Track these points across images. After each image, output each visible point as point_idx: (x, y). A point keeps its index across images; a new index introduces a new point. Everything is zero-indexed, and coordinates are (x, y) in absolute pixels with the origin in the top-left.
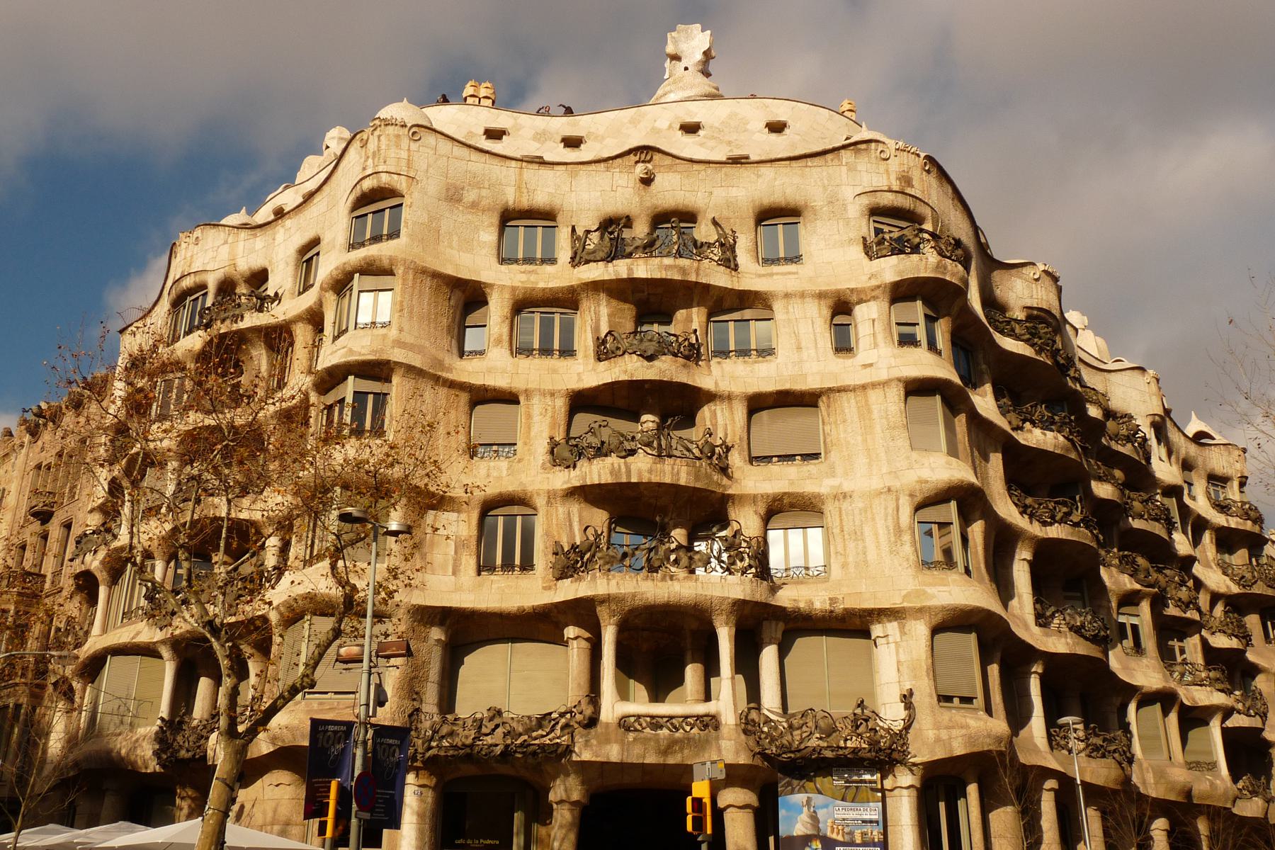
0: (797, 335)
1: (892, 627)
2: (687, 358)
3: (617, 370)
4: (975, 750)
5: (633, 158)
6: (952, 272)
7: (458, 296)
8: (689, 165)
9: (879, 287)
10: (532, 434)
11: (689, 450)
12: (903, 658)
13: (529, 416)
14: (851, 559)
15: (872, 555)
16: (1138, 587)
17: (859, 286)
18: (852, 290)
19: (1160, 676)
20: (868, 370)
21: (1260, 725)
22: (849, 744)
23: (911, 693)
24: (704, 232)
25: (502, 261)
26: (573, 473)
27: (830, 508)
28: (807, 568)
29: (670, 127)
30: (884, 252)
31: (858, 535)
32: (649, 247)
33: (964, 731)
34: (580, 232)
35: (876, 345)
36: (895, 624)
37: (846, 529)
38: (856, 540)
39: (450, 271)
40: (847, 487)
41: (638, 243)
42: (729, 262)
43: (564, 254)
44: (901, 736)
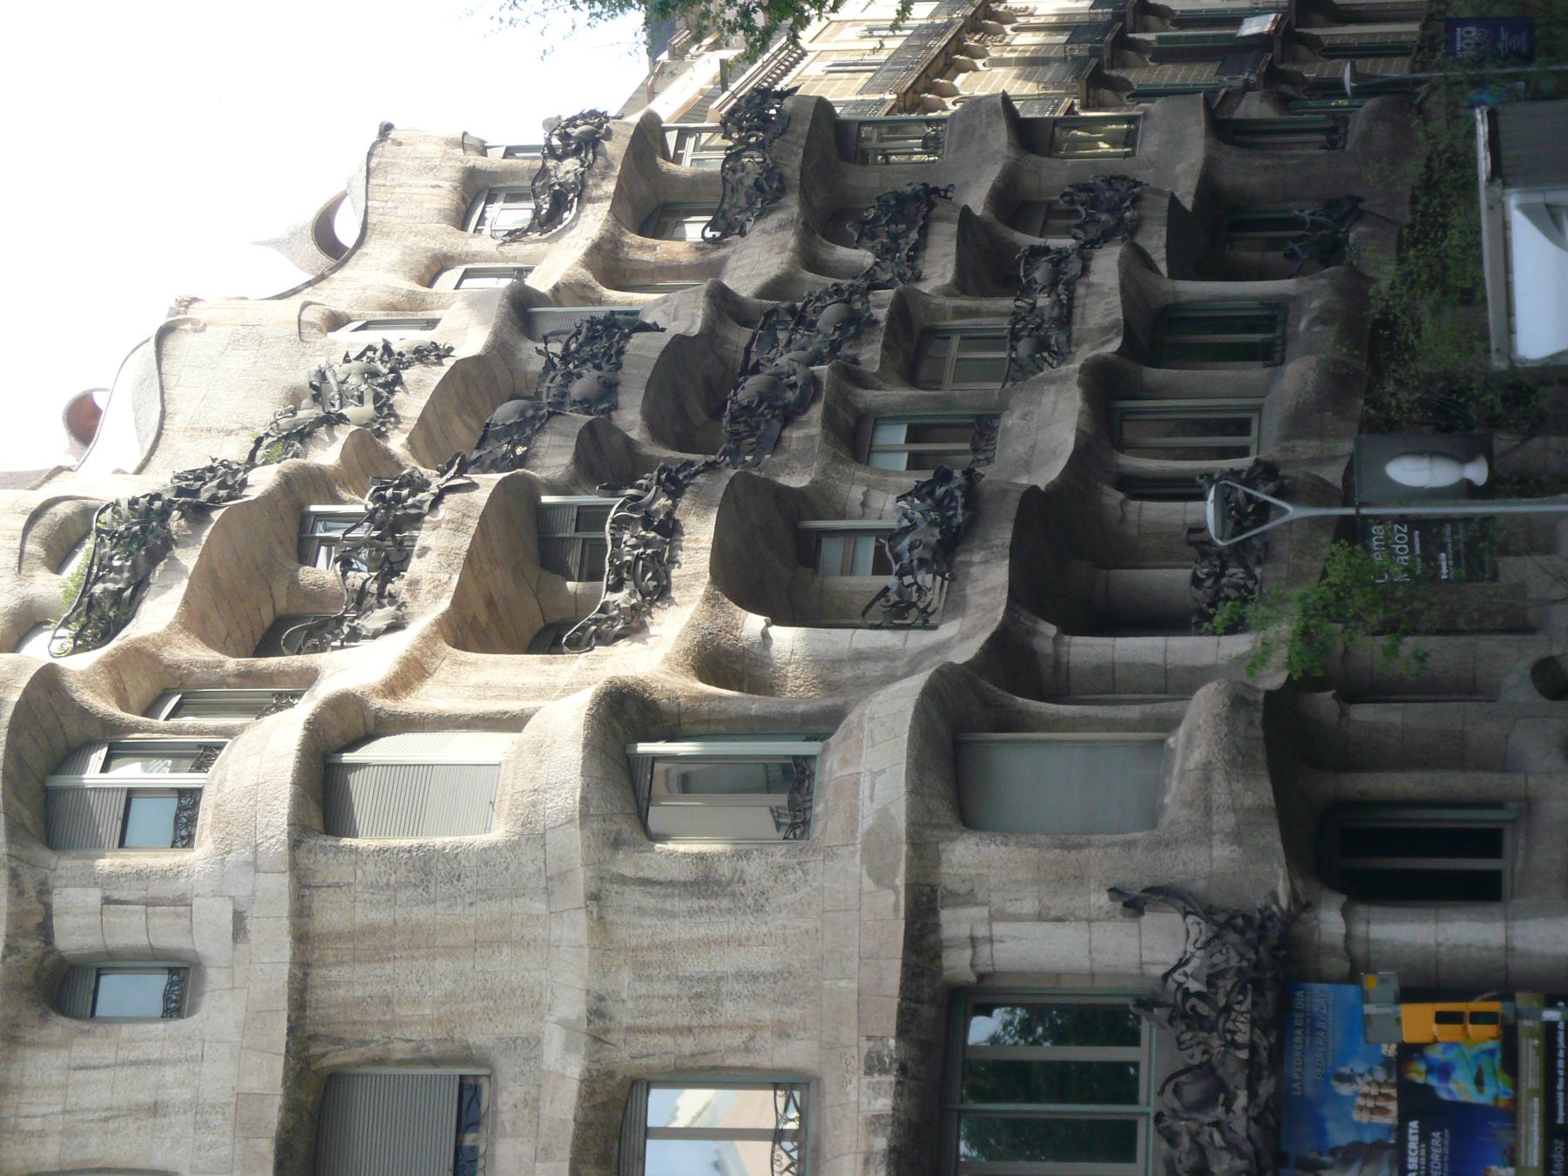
0: (113, 1114)
1: (955, 923)
4: (1261, 757)
12: (1029, 906)
14: (766, 1015)
15: (762, 959)
16: (816, 412)
19: (1049, 397)
20: (250, 924)
21: (1166, 202)
22: (1240, 1038)
23: (1115, 892)
27: (625, 1055)
28: (778, 1136)
31: (706, 992)
33: (1218, 776)
36: (945, 915)
37: (684, 1021)
38: (716, 996)
40: (571, 1005)
44: (1222, 919)
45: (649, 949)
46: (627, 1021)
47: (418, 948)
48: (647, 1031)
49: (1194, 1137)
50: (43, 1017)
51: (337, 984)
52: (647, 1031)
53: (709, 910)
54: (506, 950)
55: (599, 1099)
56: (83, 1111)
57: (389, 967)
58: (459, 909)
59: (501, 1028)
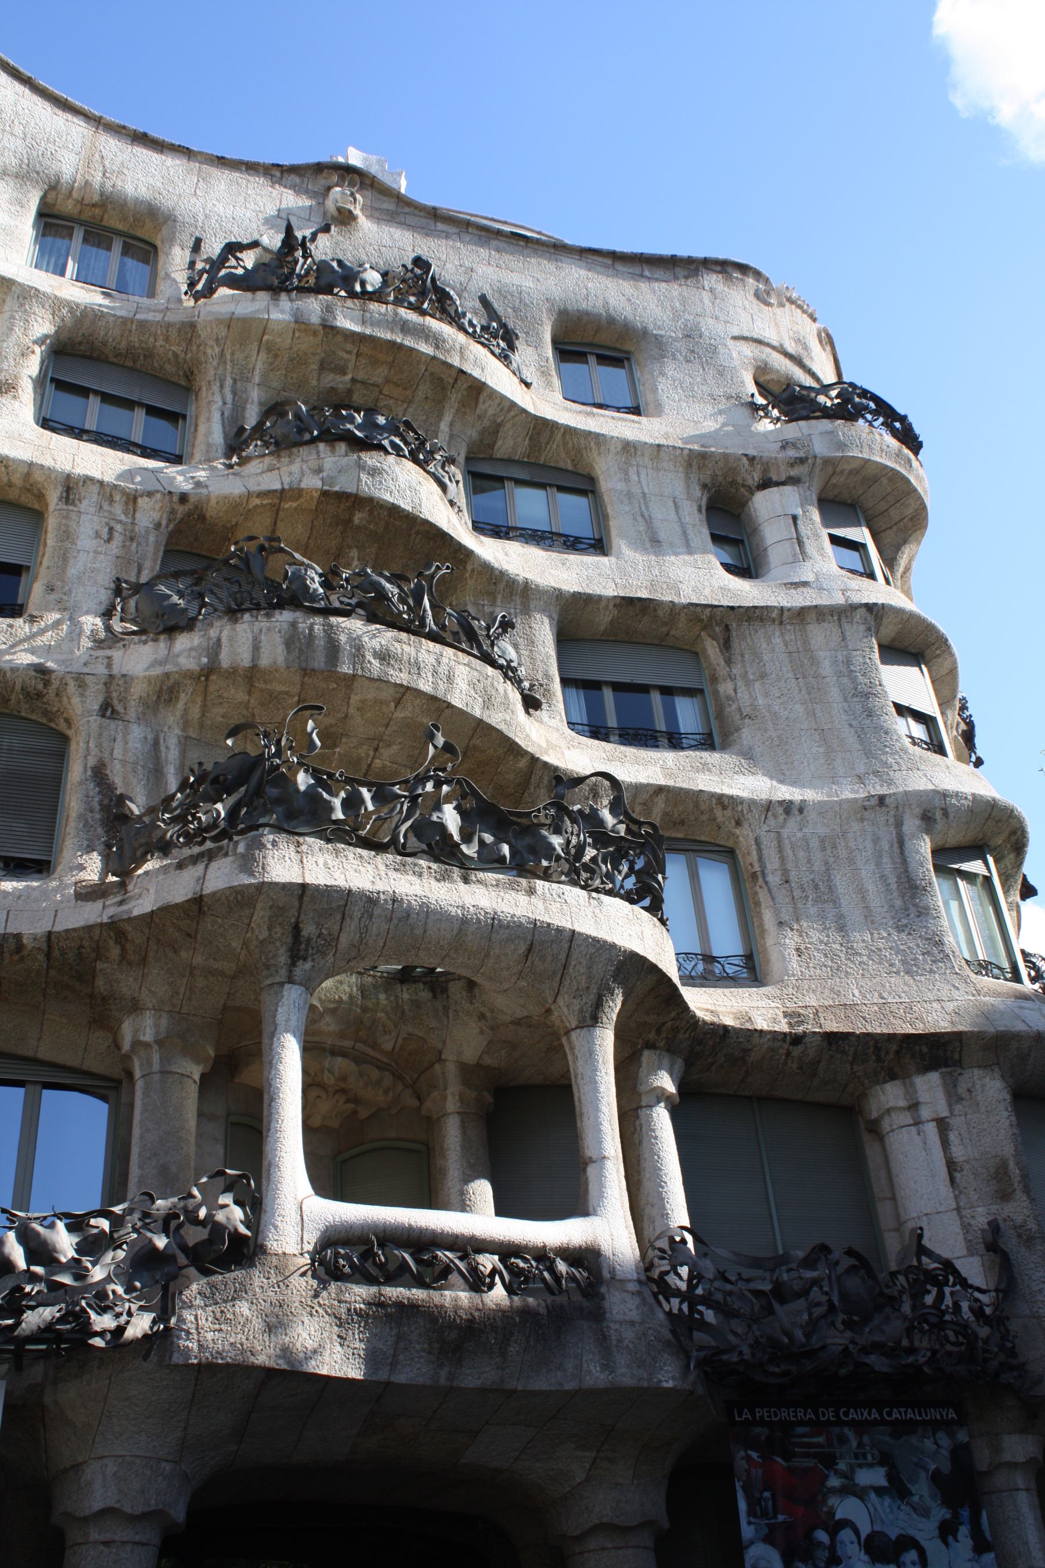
0: (648, 522)
1: (929, 1087)
3: (295, 468)
9: (802, 461)
10: (72, 571)
12: (958, 1152)
13: (67, 536)
18: (752, 459)
23: (994, 1227)
26: (184, 642)
28: (709, 959)
36: (934, 1078)
37: (793, 875)
45: (847, 847)
46: (785, 832)
47: (809, 693)
48: (780, 849)
49: (815, 1282)
50: (704, 486)
51: (769, 642)
52: (780, 849)
53: (888, 891)
54: (821, 750)
55: (718, 813)
56: (647, 508)
57: (790, 675)
58: (844, 717)
59: (758, 750)
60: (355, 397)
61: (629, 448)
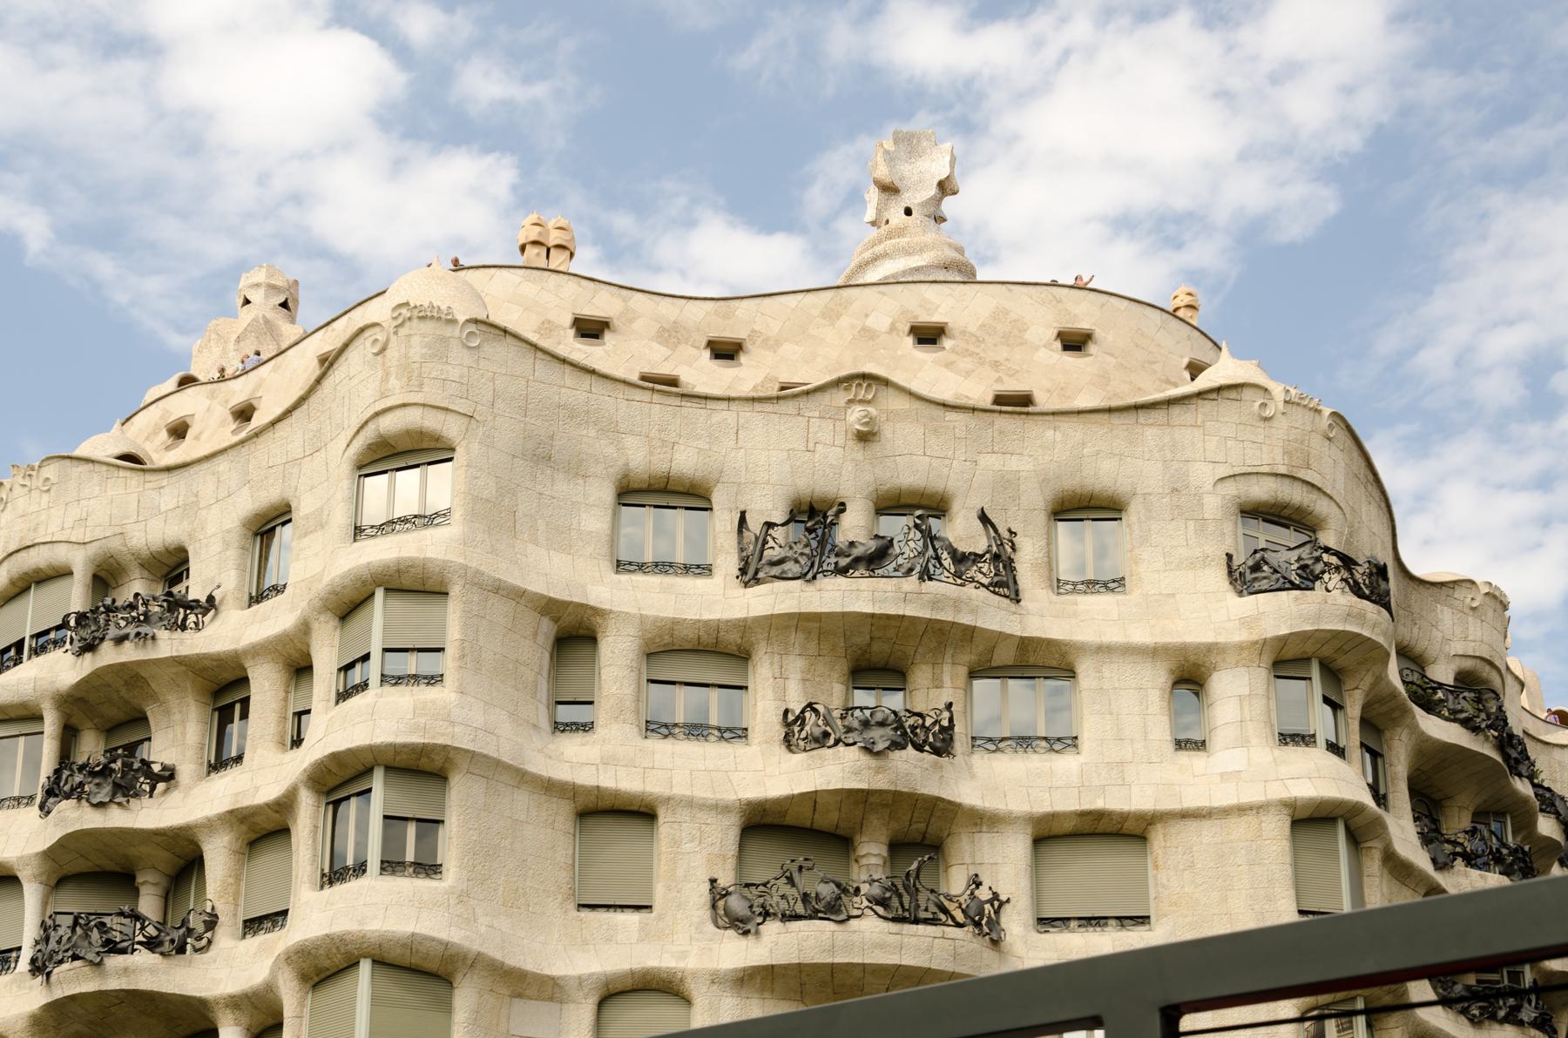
2: (937, 752)
5: (840, 397)
6: (1368, 621)
7: (547, 629)
8: (939, 412)
10: (680, 873)
11: (945, 911)
13: (676, 843)
17: (1221, 639)
24: (962, 531)
25: (620, 566)
29: (893, 328)
30: (1264, 584)
32: (876, 559)
34: (755, 525)
35: (1244, 743)
39: (537, 586)
41: (857, 552)
42: (1006, 585)
43: (727, 563)
50: (1172, 672)
60: (876, 647)
61: (1104, 651)
